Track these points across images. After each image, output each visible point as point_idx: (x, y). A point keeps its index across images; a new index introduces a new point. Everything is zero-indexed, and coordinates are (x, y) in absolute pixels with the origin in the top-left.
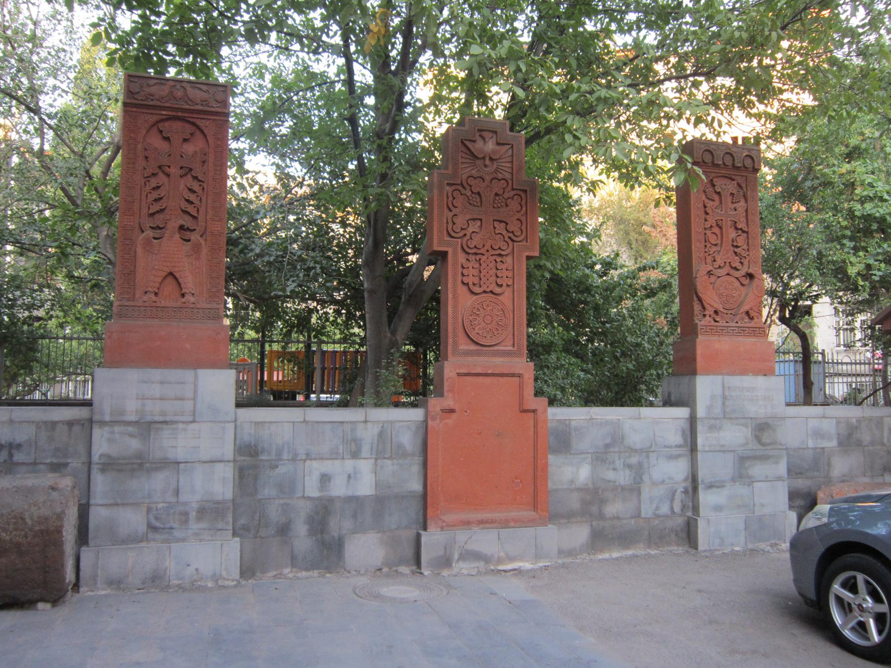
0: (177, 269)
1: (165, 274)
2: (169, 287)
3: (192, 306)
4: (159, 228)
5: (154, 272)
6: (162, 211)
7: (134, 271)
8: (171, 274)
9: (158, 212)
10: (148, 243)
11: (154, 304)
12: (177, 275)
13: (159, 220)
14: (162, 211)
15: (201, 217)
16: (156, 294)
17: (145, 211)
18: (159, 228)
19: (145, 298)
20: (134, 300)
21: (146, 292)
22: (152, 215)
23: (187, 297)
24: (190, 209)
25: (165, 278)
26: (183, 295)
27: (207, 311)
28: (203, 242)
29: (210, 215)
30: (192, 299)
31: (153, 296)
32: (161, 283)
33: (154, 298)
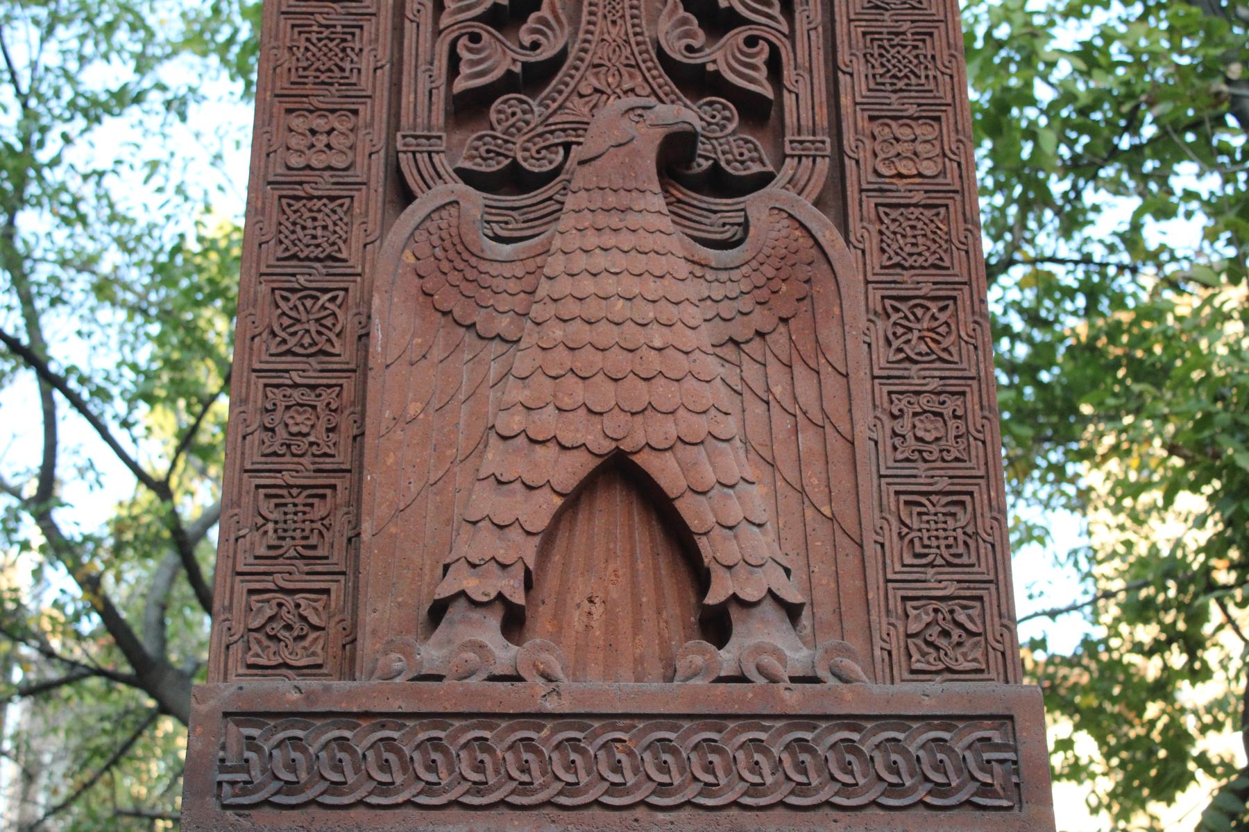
0: (662, 430)
1: (568, 471)
2: (612, 560)
3: (793, 699)
4: (515, 179)
5: (494, 459)
6: (534, 78)
7: (355, 471)
8: (620, 472)
9: (509, 83)
10: (457, 255)
11: (506, 697)
12: (667, 472)
13: (518, 128)
14: (534, 78)
15: (801, 104)
16: (514, 622)
17: (425, 97)
18: (515, 179)
19: (431, 654)
20: (348, 668)
21: (438, 611)
22: (469, 108)
23: (760, 638)
24: (721, 56)
25: (575, 500)
26: (716, 626)
27: (916, 741)
28: (828, 234)
29: (854, 89)
30: (795, 653)
31: (489, 630)
32: (548, 537)
33: (504, 654)
